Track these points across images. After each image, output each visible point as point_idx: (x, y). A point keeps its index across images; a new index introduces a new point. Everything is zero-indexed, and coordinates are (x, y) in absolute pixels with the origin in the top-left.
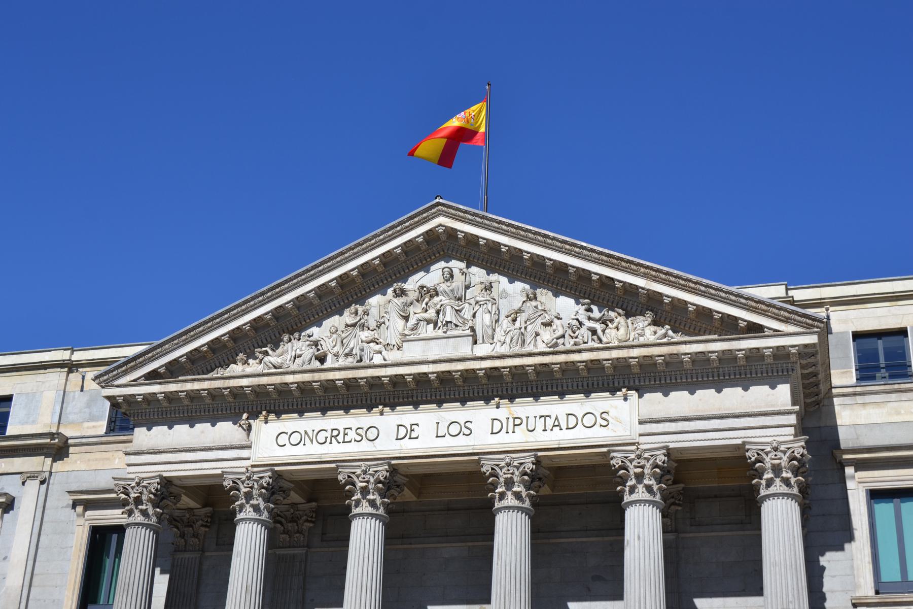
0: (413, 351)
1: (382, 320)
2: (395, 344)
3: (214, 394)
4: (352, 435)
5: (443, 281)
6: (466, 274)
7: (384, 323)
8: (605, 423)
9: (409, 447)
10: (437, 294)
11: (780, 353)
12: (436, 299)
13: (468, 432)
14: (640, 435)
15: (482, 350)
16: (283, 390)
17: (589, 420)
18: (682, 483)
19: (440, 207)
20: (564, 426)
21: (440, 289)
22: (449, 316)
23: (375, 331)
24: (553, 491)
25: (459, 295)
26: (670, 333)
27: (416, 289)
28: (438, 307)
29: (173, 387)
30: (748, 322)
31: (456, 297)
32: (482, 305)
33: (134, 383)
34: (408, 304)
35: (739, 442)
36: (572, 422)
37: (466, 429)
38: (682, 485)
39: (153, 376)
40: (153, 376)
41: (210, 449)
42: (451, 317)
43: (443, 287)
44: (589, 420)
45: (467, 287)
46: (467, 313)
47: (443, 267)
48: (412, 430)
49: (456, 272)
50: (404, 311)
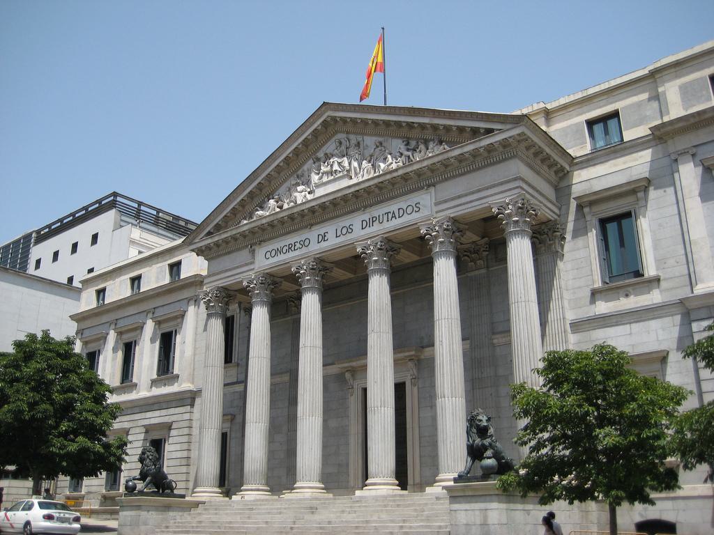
0: (320, 192)
3: (234, 238)
4: (298, 245)
8: (417, 209)
9: (324, 245)
10: (333, 156)
11: (505, 144)
12: (332, 160)
13: (350, 231)
14: (437, 212)
15: (354, 181)
16: (262, 229)
17: (409, 210)
18: (487, 237)
20: (397, 216)
22: (336, 167)
24: (420, 255)
26: (446, 146)
27: (322, 155)
29: (216, 239)
30: (486, 129)
33: (202, 240)
35: (487, 205)
36: (401, 211)
37: (350, 230)
38: (487, 239)
39: (209, 233)
40: (209, 233)
41: (237, 267)
44: (409, 210)
48: (325, 236)
49: (342, 140)
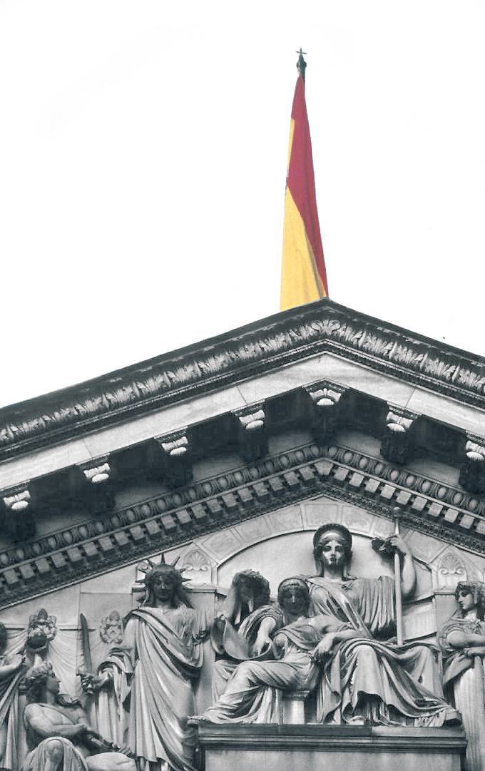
1: (104, 677)
2: (161, 754)
5: (314, 571)
6: (402, 556)
7: (109, 686)
19: (328, 326)
21: (318, 594)
23: (79, 712)
25: (380, 622)
27: (225, 582)
28: (324, 645)
31: (369, 626)
32: (477, 659)
34: (195, 633)
42: (379, 682)
43: (326, 587)
45: (410, 600)
46: (428, 677)
47: (317, 528)
49: (360, 546)
50: (190, 653)
